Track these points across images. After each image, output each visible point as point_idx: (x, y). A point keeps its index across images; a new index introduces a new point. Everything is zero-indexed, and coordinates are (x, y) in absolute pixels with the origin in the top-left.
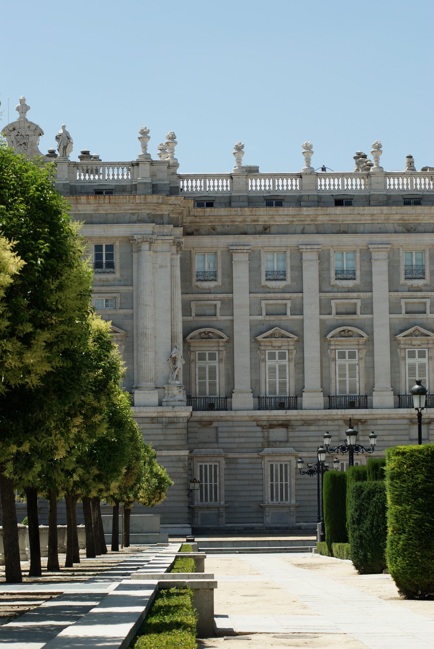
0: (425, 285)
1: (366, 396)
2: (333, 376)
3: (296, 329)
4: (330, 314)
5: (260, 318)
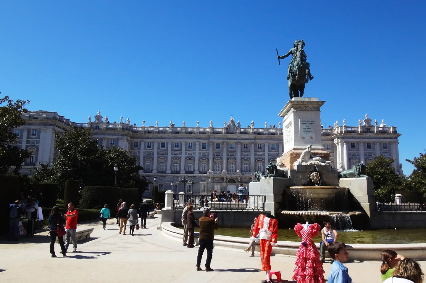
3: (180, 158)
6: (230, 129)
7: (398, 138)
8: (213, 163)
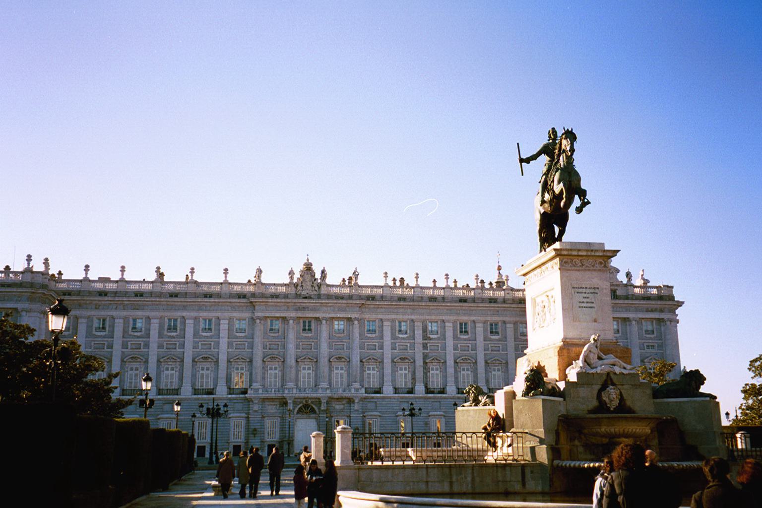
0: (177, 335)
1: (178, 389)
2: (126, 379)
4: (127, 348)
5: (90, 350)
6: (302, 286)
7: (677, 312)
8: (263, 368)
